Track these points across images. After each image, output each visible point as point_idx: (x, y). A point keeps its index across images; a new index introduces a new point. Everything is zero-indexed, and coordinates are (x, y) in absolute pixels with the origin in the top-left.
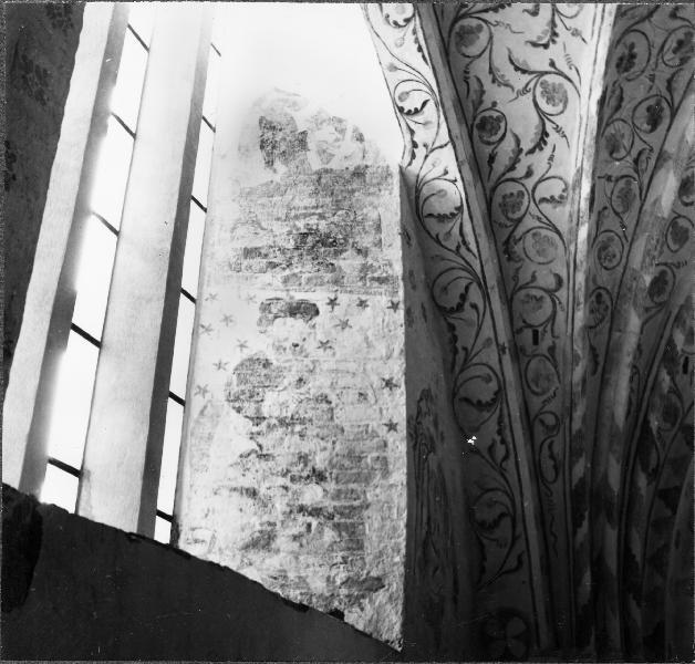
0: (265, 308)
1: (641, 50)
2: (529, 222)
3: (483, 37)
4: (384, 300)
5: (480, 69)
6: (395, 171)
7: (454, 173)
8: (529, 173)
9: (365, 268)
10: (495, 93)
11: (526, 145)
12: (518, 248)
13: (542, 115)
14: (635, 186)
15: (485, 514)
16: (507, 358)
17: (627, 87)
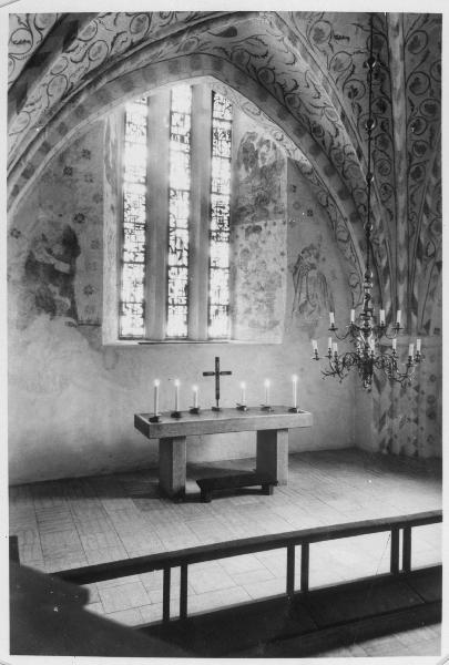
0: (247, 230)
1: (357, 85)
2: (347, 164)
3: (297, 100)
4: (281, 221)
5: (302, 111)
6: (286, 161)
7: (305, 158)
8: (339, 145)
9: (275, 208)
10: (313, 118)
11: (333, 134)
12: (347, 174)
13: (333, 122)
14: (387, 137)
15: (353, 283)
16: (349, 223)
17: (360, 102)
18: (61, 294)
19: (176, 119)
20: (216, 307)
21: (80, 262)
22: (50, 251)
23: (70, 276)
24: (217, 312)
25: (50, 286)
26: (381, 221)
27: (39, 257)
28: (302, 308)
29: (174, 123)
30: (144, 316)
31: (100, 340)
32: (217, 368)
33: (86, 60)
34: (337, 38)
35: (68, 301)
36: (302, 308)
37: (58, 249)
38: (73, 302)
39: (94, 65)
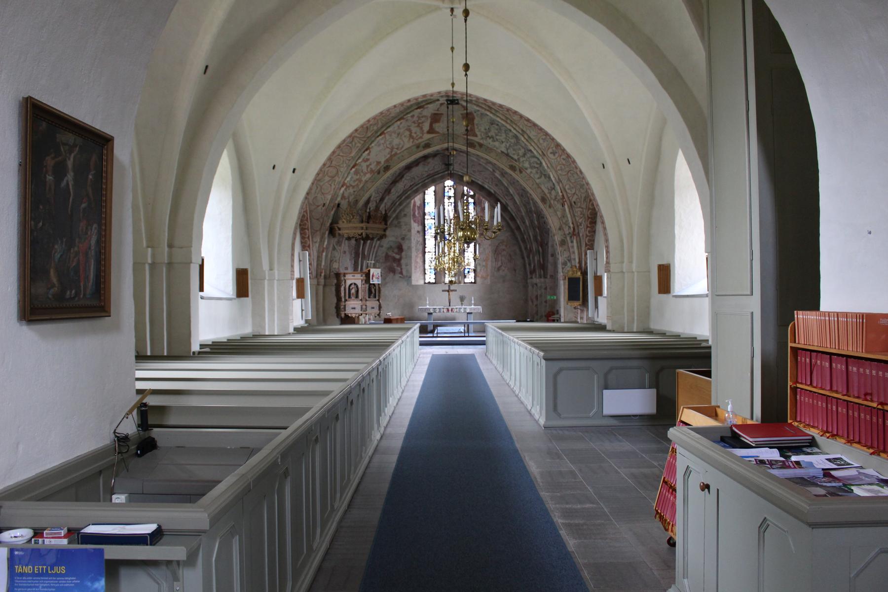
18: (397, 266)
19: (447, 189)
20: (468, 270)
21: (403, 254)
22: (393, 251)
23: (399, 260)
24: (469, 272)
25: (394, 263)
26: (524, 231)
27: (390, 253)
28: (499, 269)
29: (446, 191)
30: (435, 274)
31: (411, 283)
32: (452, 291)
33: (397, 194)
34: (481, 171)
35: (399, 269)
36: (499, 269)
37: (396, 250)
38: (401, 269)
39: (399, 195)
